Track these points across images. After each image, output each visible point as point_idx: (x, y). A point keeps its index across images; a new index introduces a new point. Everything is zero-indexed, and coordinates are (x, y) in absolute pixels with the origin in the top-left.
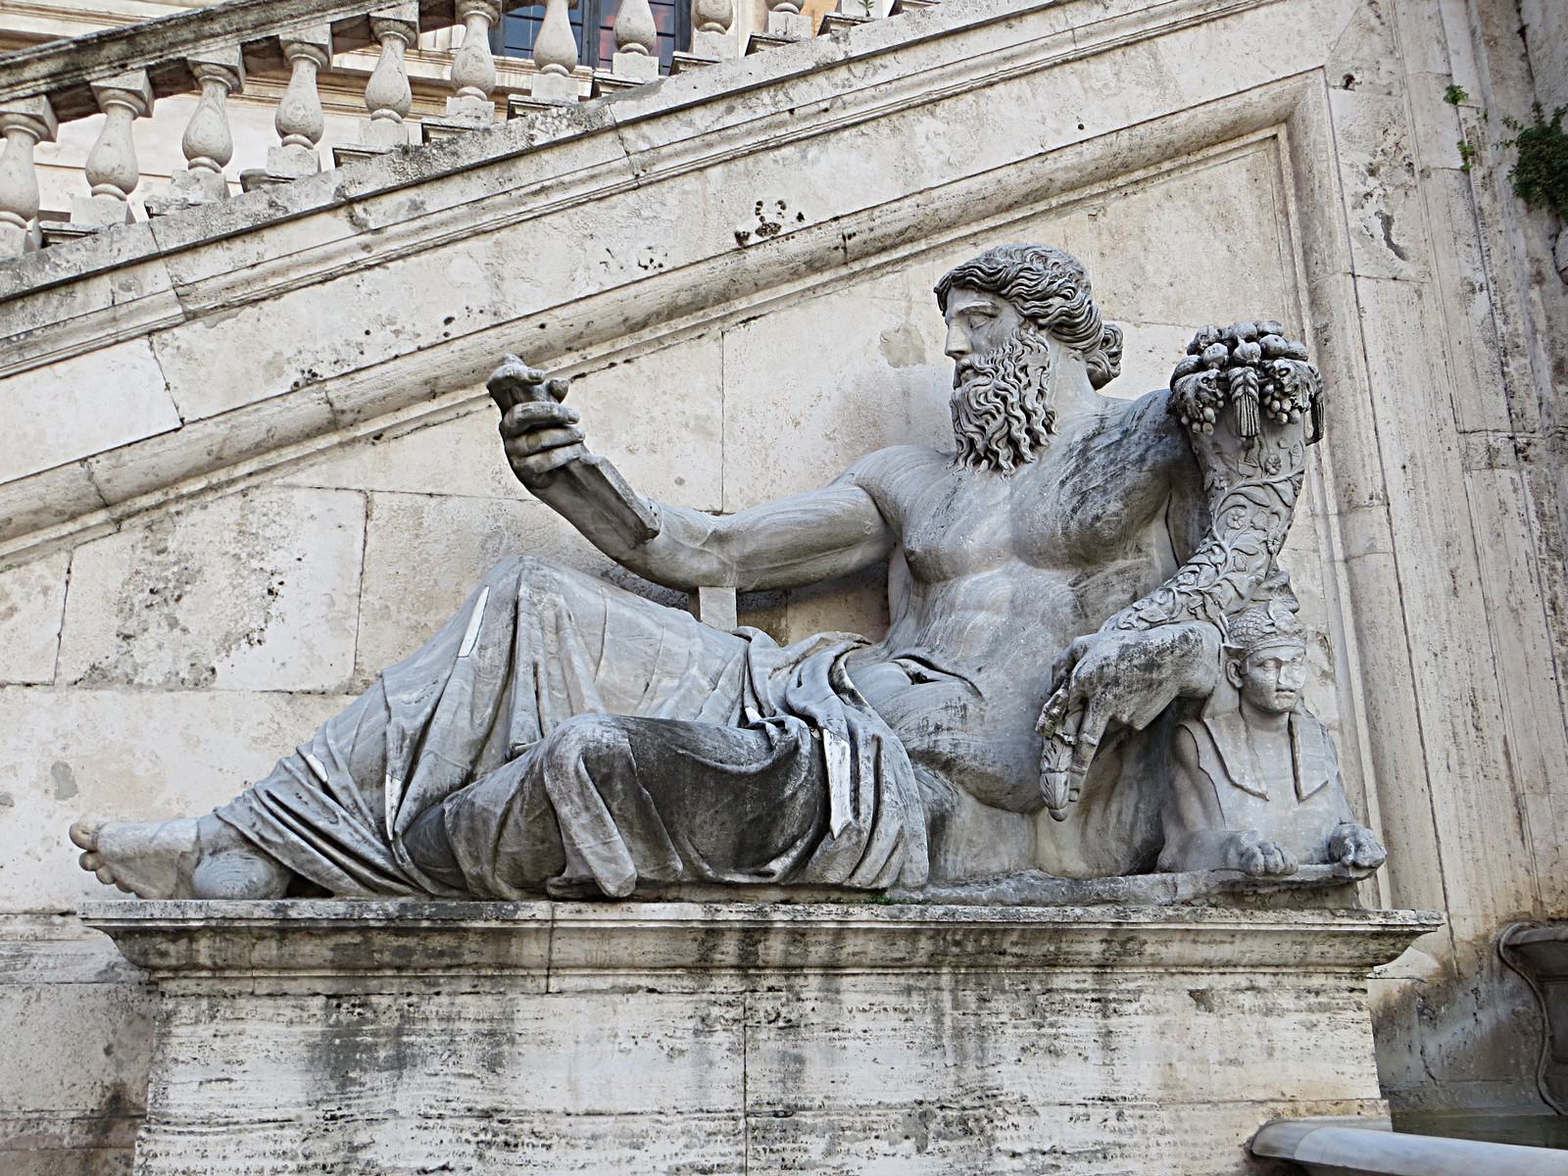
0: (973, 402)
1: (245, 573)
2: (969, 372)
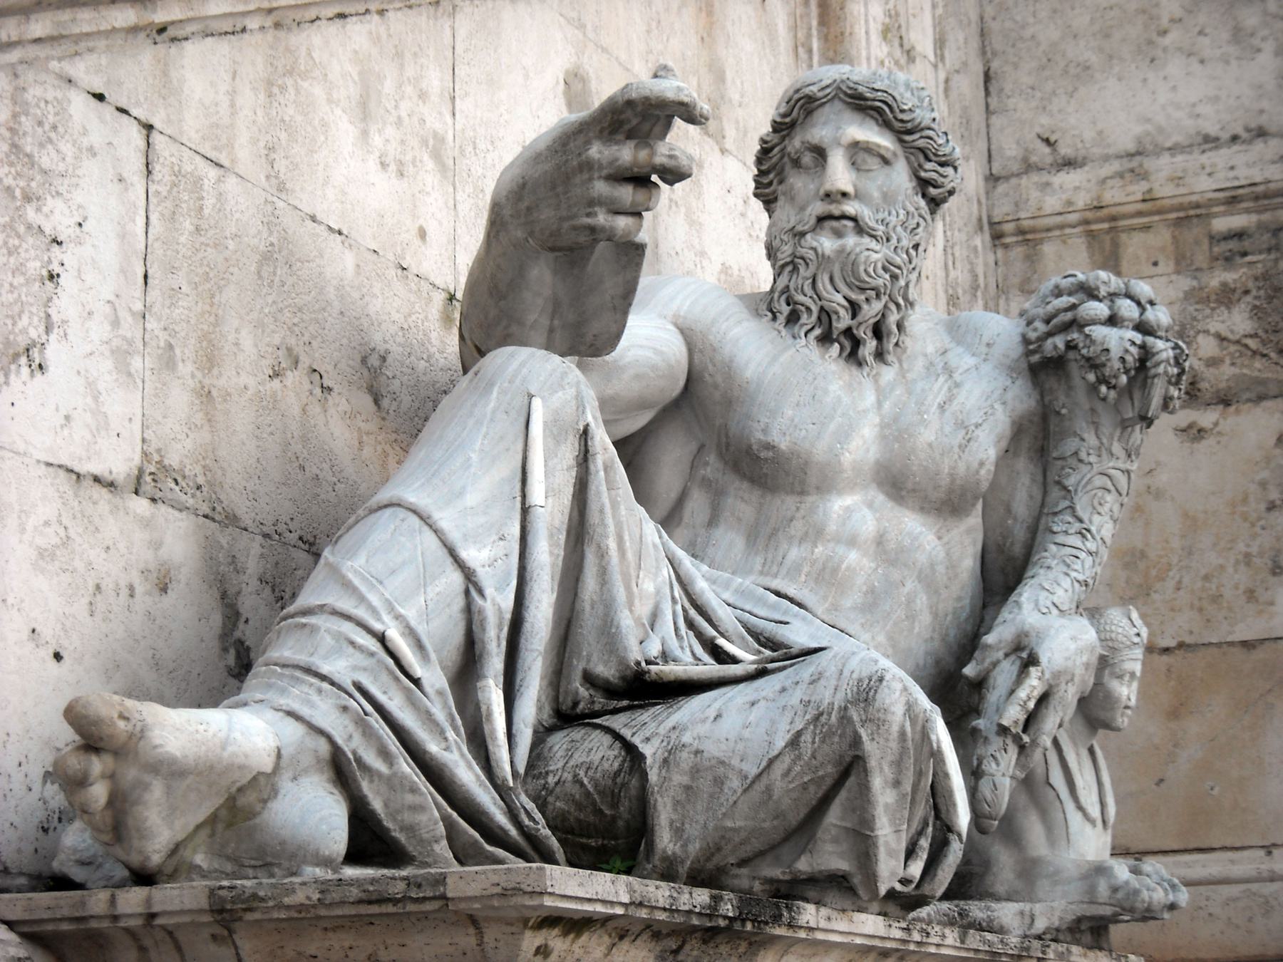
0: (862, 268)
1: (22, 229)
2: (850, 224)
